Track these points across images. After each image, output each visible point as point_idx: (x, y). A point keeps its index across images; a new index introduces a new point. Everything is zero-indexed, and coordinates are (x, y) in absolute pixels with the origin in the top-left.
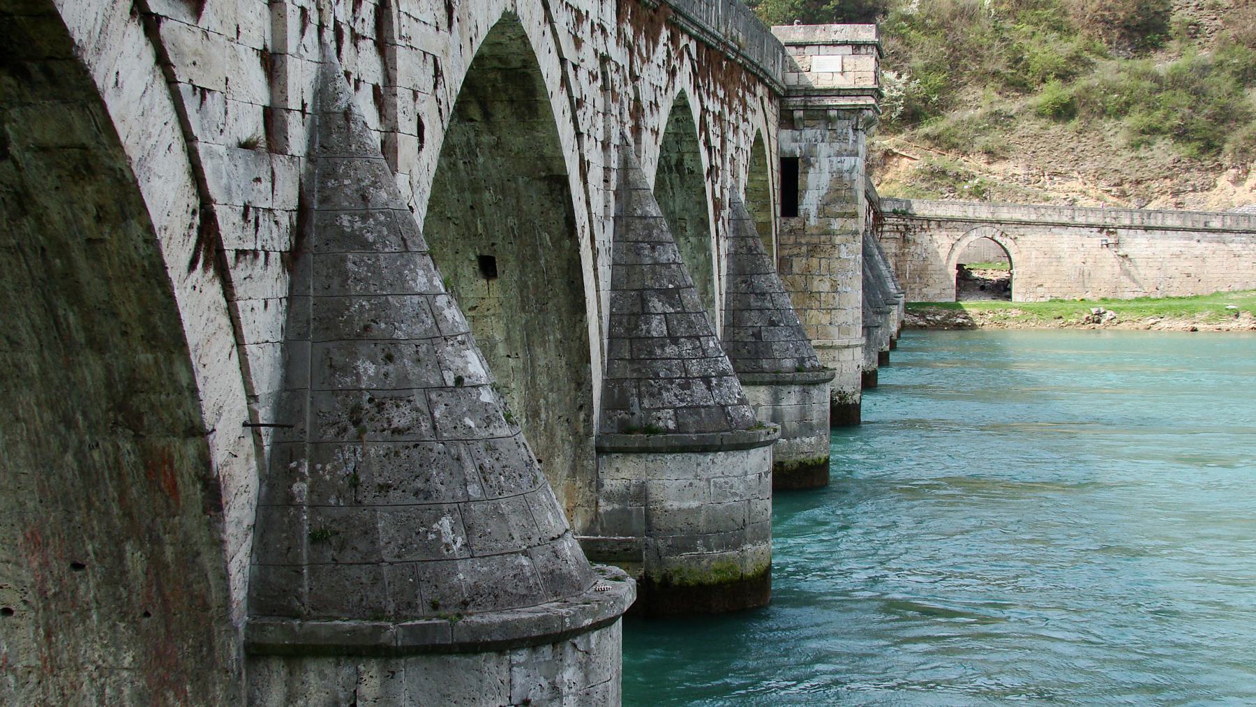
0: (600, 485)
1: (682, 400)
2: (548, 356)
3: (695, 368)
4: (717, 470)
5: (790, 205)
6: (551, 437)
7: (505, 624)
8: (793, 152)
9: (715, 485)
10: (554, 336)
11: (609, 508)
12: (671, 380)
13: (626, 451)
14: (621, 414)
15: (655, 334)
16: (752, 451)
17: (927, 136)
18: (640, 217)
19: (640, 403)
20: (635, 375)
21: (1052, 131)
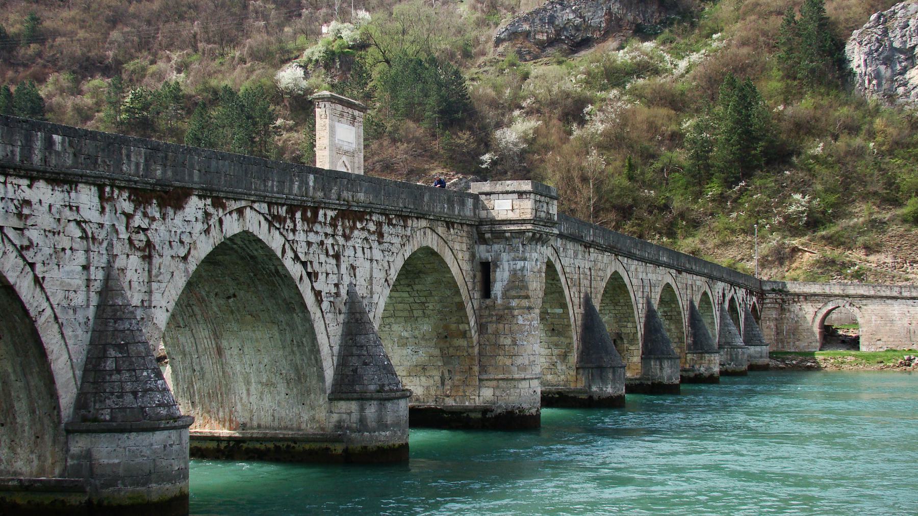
0: (68, 450)
1: (117, 404)
2: (35, 381)
3: (128, 387)
4: (131, 443)
5: (486, 290)
6: (42, 425)
8: (487, 259)
9: (129, 451)
10: (36, 370)
11: (72, 463)
12: (112, 393)
13: (81, 432)
14: (83, 412)
15: (107, 368)
16: (158, 433)
17: (823, 237)
18: (111, 306)
19: (95, 405)
20: (94, 391)
21: (913, 232)
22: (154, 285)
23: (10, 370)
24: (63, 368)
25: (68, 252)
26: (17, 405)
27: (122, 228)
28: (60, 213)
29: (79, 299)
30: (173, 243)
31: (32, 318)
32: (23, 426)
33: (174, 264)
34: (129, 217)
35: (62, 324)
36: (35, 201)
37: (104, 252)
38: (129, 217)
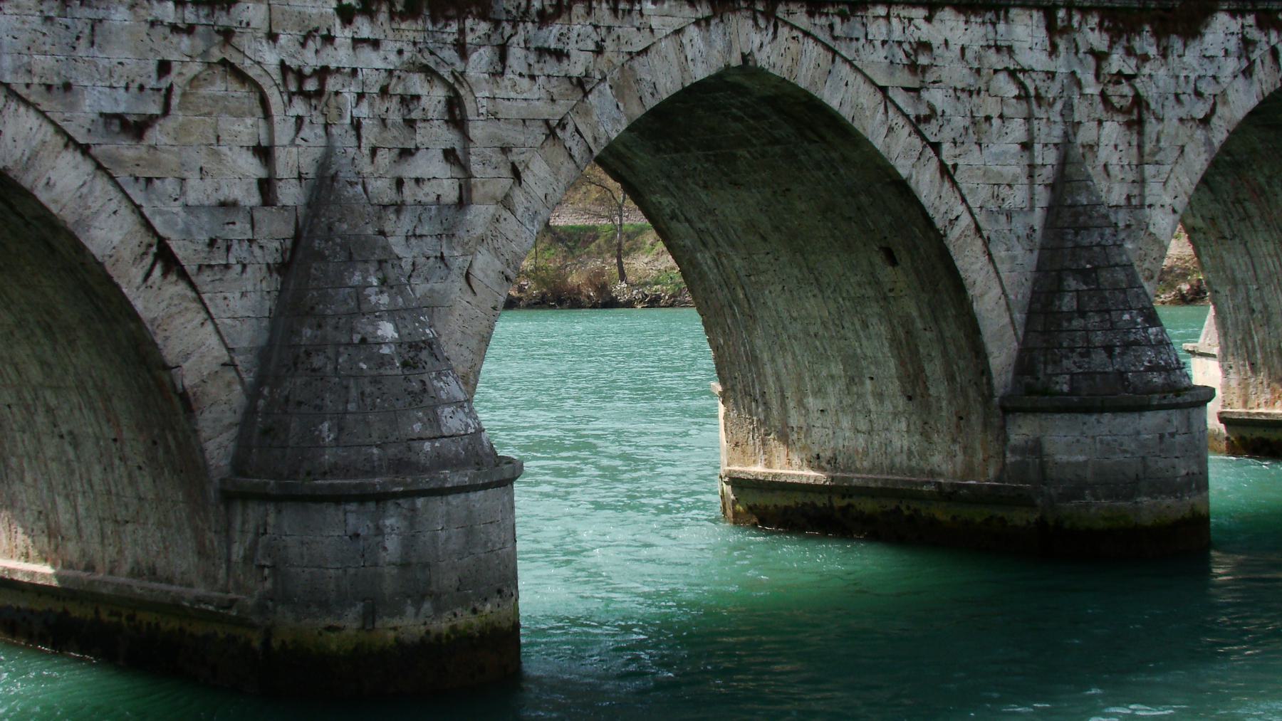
0: (1006, 440)
2: (951, 329)
3: (1098, 338)
6: (966, 397)
7: (331, 485)
9: (1101, 442)
10: (951, 312)
11: (1013, 460)
12: (1072, 350)
13: (1025, 411)
14: (1028, 379)
15: (1064, 309)
16: (1148, 414)
18: (1070, 206)
19: (1045, 368)
20: (1045, 345)
22: (1149, 170)
23: (915, 314)
24: (993, 310)
25: (996, 122)
26: (928, 368)
27: (1088, 77)
28: (979, 58)
29: (1017, 198)
30: (1183, 97)
31: (938, 230)
32: (938, 399)
33: (1184, 132)
34: (1100, 57)
35: (989, 238)
36: (936, 42)
37: (1058, 119)
38: (1100, 57)
